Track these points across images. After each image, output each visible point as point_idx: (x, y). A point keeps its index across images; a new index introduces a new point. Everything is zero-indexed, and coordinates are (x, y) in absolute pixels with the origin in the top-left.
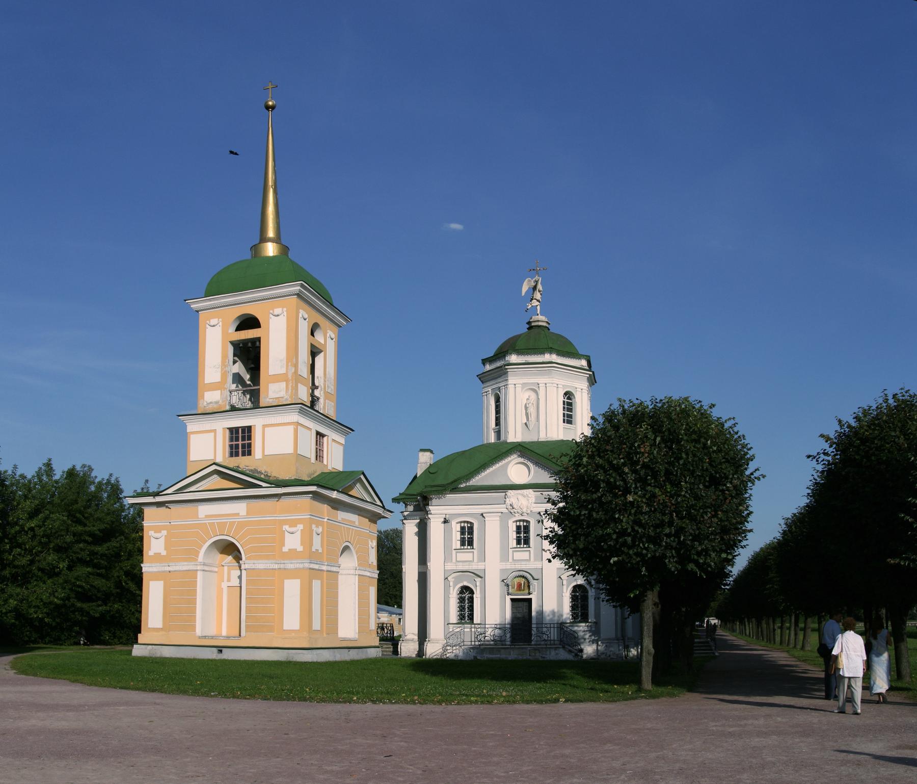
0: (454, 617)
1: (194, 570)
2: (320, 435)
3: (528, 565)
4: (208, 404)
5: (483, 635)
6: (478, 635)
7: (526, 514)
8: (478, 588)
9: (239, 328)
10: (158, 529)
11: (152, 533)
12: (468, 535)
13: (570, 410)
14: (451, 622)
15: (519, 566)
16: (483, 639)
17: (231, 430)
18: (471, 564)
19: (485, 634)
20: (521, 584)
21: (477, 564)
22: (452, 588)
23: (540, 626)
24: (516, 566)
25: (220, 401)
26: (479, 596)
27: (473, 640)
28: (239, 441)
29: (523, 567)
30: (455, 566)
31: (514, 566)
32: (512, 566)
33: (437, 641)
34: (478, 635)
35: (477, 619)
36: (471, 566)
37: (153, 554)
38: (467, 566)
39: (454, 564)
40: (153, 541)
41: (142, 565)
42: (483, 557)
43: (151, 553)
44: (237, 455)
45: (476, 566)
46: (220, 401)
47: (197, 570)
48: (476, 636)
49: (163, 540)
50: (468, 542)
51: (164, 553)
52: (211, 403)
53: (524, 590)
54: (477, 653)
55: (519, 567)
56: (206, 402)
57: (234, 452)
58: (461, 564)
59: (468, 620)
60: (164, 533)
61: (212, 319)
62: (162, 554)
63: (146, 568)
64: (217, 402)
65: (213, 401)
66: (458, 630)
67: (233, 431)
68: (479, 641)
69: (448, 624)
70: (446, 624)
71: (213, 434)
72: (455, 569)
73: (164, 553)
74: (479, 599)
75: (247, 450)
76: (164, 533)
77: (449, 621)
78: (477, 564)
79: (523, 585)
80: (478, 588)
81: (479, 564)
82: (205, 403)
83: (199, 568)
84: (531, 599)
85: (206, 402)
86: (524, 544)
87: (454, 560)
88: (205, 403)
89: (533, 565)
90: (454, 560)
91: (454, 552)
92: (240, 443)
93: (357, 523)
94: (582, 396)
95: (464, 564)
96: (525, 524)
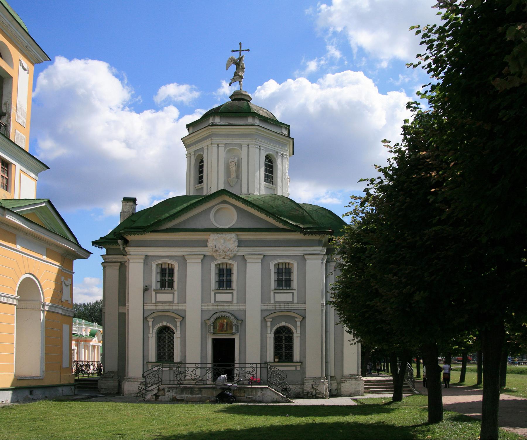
0: (152, 356)
5: (183, 375)
6: (177, 375)
8: (179, 329)
12: (168, 277)
13: (271, 172)
14: (150, 360)
15: (222, 307)
16: (182, 379)
18: (171, 305)
19: (185, 373)
20: (224, 325)
21: (177, 305)
22: (151, 329)
23: (242, 365)
24: (219, 307)
27: (172, 379)
29: (226, 308)
30: (155, 307)
31: (216, 307)
32: (215, 307)
33: (134, 380)
34: (177, 375)
36: (171, 307)
38: (168, 307)
39: (154, 305)
42: (183, 299)
45: (177, 307)
48: (175, 375)
50: (169, 283)
53: (226, 331)
54: (176, 393)
55: (220, 308)
58: (161, 304)
66: (156, 369)
68: (179, 381)
69: (147, 362)
70: (145, 362)
72: (155, 309)
74: (179, 340)
77: (148, 359)
78: (177, 305)
79: (225, 325)
80: (179, 329)
81: (180, 305)
84: (234, 340)
86: (227, 287)
87: (153, 301)
89: (237, 307)
90: (153, 301)
95: (164, 305)
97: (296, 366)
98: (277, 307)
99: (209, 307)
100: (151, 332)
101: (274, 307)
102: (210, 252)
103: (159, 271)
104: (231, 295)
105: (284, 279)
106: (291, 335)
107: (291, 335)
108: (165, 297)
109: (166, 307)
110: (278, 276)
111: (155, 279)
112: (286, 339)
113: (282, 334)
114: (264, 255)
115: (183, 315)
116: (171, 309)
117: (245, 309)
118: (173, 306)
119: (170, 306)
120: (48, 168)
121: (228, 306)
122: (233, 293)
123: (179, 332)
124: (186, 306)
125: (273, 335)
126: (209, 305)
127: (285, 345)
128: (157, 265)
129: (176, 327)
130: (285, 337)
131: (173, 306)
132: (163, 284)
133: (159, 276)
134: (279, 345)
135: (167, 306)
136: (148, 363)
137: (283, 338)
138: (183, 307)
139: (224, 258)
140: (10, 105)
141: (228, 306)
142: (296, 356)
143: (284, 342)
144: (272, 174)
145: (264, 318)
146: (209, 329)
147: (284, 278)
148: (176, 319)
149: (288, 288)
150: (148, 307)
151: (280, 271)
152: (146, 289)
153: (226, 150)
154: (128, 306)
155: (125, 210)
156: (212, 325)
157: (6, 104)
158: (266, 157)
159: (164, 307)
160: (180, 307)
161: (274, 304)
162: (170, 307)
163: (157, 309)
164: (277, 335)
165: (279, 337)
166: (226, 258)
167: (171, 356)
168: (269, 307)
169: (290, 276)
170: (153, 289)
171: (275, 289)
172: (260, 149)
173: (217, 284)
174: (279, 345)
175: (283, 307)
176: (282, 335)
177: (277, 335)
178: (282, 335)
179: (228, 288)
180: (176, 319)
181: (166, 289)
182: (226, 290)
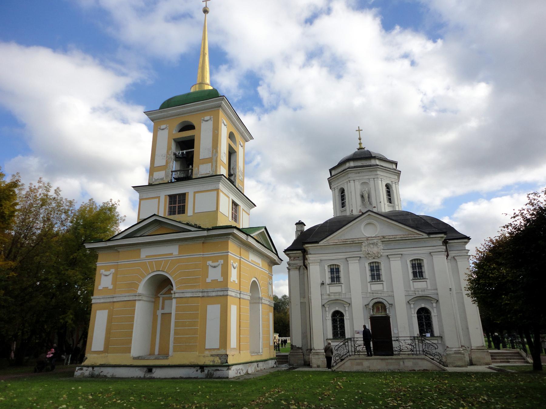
0: (330, 335)
1: (134, 300)
2: (235, 204)
3: (383, 294)
4: (156, 180)
7: (377, 258)
8: (347, 312)
9: (181, 130)
10: (108, 268)
11: (103, 271)
17: (171, 197)
24: (374, 295)
25: (165, 178)
26: (348, 318)
28: (176, 204)
31: (372, 295)
32: (371, 295)
33: (317, 354)
35: (348, 335)
36: (340, 296)
37: (102, 289)
38: (338, 296)
40: (103, 278)
41: (92, 298)
43: (100, 288)
44: (174, 213)
45: (345, 296)
46: (165, 178)
47: (135, 300)
49: (110, 277)
51: (111, 287)
52: (158, 179)
55: (376, 296)
56: (154, 179)
57: (172, 212)
59: (340, 336)
60: (113, 270)
61: (162, 125)
62: (109, 288)
63: (95, 300)
64: (162, 179)
65: (159, 178)
67: (172, 198)
69: (327, 339)
70: (325, 339)
71: (157, 200)
73: (111, 287)
75: (182, 210)
76: (113, 270)
77: (327, 337)
79: (380, 308)
82: (154, 180)
83: (137, 298)
85: (154, 179)
88: (154, 180)
89: (387, 294)
91: (328, 286)
92: (177, 205)
93: (261, 266)
94: (396, 186)
95: (335, 295)
96: (377, 265)
97: (437, 340)
98: (416, 292)
99: (367, 295)
100: (327, 316)
101: (414, 293)
102: (364, 254)
103: (330, 270)
104: (382, 285)
105: (417, 271)
106: (429, 314)
107: (429, 314)
108: (335, 289)
109: (337, 296)
110: (413, 269)
111: (328, 275)
112: (426, 318)
113: (422, 314)
114: (402, 255)
115: (349, 302)
116: (341, 297)
117: (393, 295)
118: (341, 295)
119: (340, 295)
120: (255, 206)
121: (381, 293)
122: (383, 283)
123: (347, 315)
124: (351, 295)
125: (416, 315)
126: (367, 293)
127: (426, 323)
128: (328, 266)
129: (345, 311)
130: (425, 316)
131: (341, 295)
132: (332, 279)
133: (330, 273)
134: (421, 323)
135: (337, 295)
136: (327, 340)
137: (423, 317)
138: (349, 296)
139: (374, 258)
140: (235, 169)
141: (381, 293)
142: (437, 333)
143: (424, 320)
144: (390, 197)
145: (408, 302)
146: (369, 312)
147: (417, 270)
148: (345, 305)
149: (422, 278)
150: (324, 297)
151: (414, 265)
152: (323, 284)
153: (360, 183)
154: (311, 297)
155: (298, 229)
156: (372, 308)
157: (233, 169)
158: (386, 186)
159: (335, 296)
160: (346, 296)
161: (414, 291)
162: (339, 296)
163: (331, 298)
164: (419, 315)
165: (420, 316)
166: (375, 258)
167: (343, 334)
168: (410, 293)
169: (421, 269)
170: (327, 284)
171: (413, 279)
172: (382, 181)
173: (370, 277)
174: (421, 323)
175: (421, 292)
176: (422, 315)
177: (419, 315)
178: (422, 315)
179: (379, 280)
180: (345, 305)
181: (335, 283)
182: (377, 281)
